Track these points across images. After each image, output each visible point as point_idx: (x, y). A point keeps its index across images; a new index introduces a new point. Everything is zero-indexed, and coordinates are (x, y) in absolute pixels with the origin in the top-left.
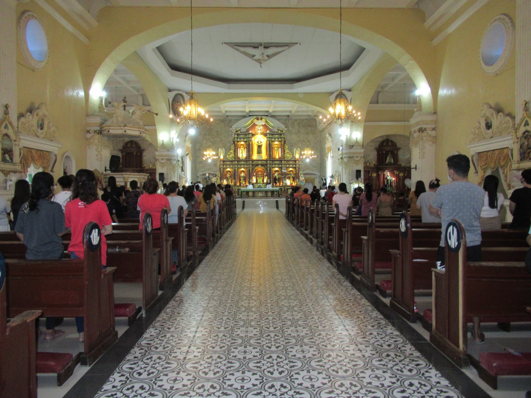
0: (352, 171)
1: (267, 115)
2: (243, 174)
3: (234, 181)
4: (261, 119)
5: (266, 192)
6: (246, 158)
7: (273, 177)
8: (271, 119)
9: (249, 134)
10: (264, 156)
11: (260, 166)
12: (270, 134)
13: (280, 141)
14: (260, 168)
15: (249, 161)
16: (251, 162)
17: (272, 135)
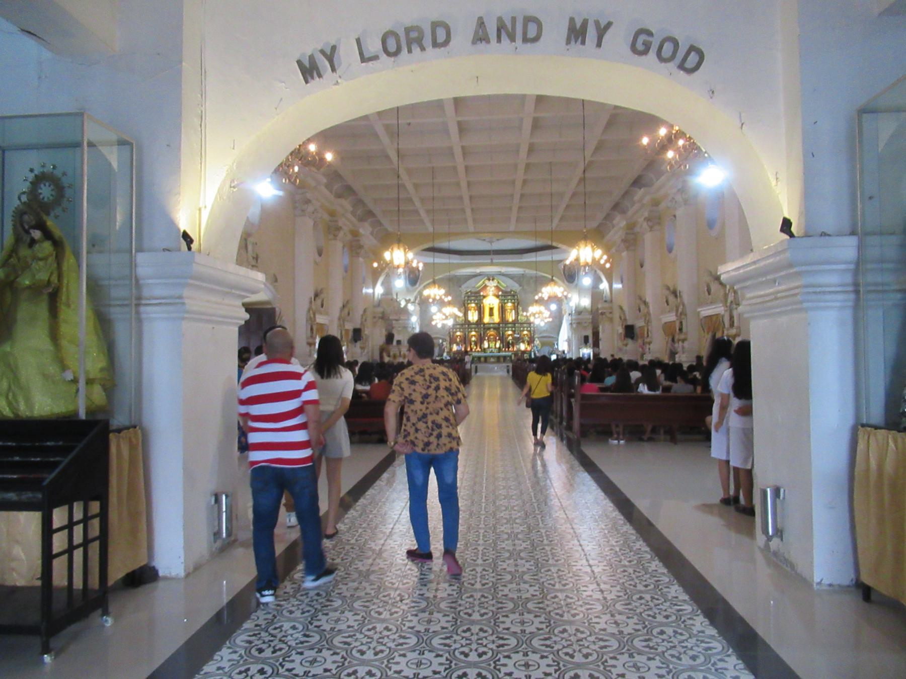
0: (581, 337)
2: (473, 339)
3: (464, 346)
4: (493, 280)
5: (498, 357)
6: (477, 321)
7: (506, 340)
8: (504, 278)
9: (480, 296)
10: (496, 319)
11: (492, 330)
12: (502, 296)
13: (514, 303)
14: (492, 332)
15: (481, 324)
16: (482, 326)
17: (505, 296)
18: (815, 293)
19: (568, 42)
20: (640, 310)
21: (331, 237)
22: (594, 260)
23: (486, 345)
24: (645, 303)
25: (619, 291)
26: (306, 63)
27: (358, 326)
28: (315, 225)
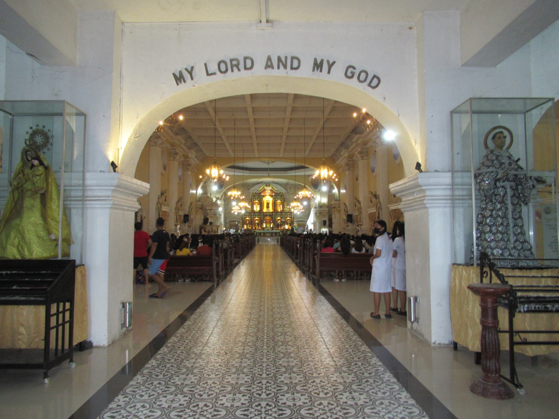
1: (274, 182)
2: (257, 222)
3: (251, 226)
4: (269, 186)
5: (272, 233)
6: (259, 211)
8: (274, 184)
9: (261, 196)
10: (271, 209)
13: (281, 200)
14: (268, 218)
17: (276, 196)
18: (432, 199)
19: (313, 70)
20: (355, 206)
21: (171, 158)
22: (328, 175)
23: (264, 226)
24: (359, 201)
25: (343, 194)
26: (178, 75)
27: (187, 213)
28: (162, 152)
